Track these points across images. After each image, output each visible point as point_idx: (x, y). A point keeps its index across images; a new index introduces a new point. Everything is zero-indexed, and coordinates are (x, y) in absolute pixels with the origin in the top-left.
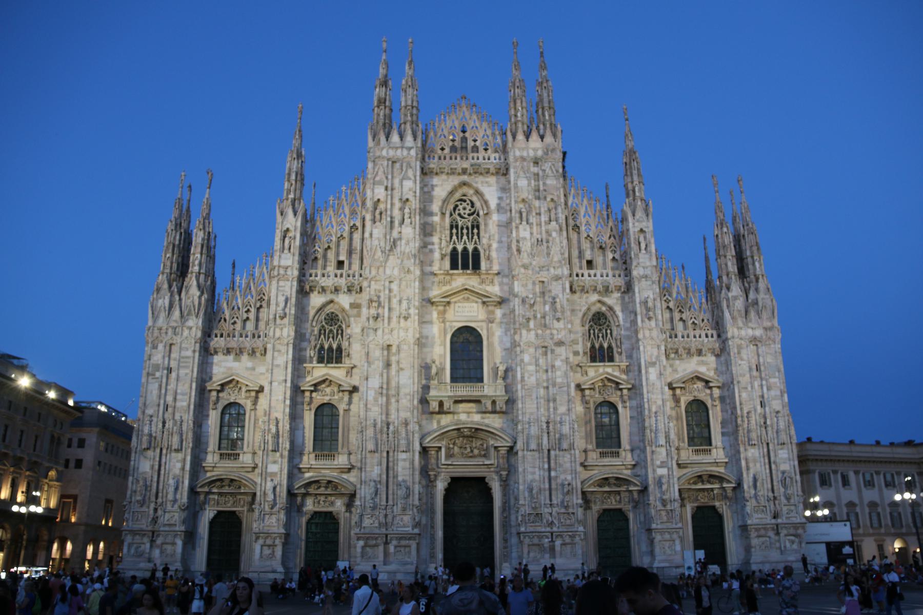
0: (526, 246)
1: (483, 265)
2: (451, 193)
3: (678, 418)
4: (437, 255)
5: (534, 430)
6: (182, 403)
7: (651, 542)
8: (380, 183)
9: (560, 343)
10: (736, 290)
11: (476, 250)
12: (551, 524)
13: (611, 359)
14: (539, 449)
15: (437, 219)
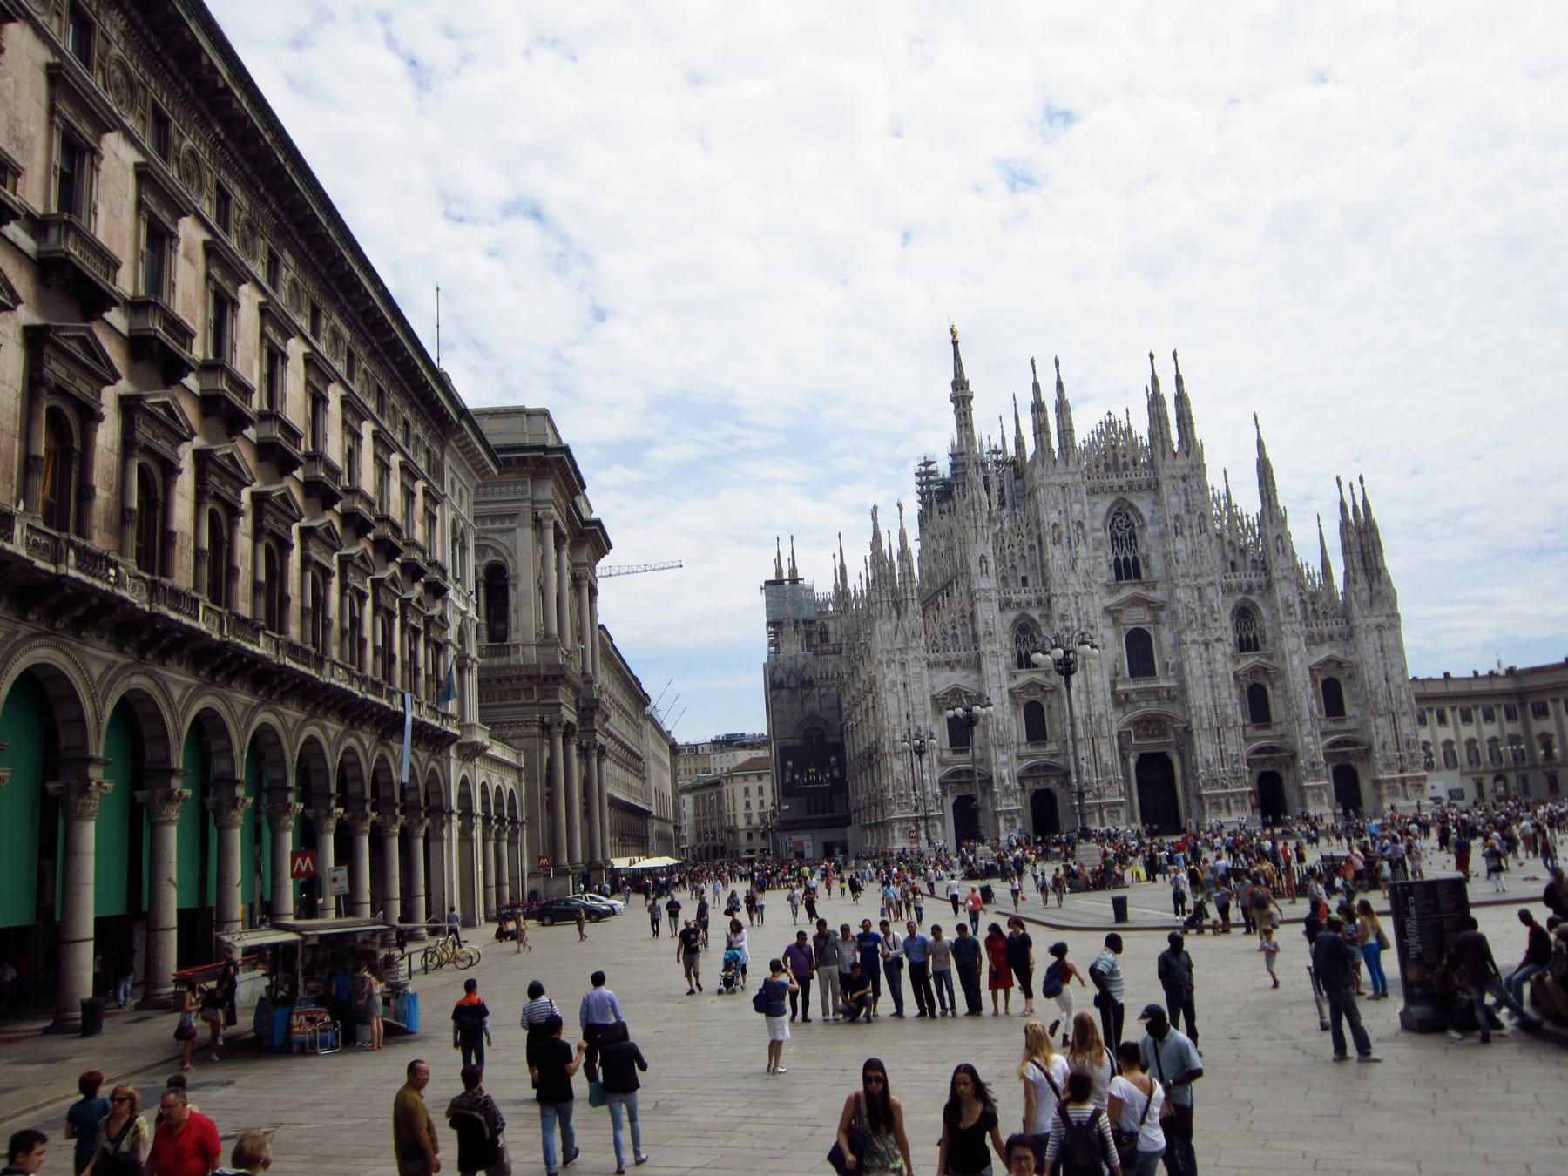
0: (1183, 556)
1: (1143, 572)
2: (1110, 510)
3: (1316, 694)
4: (1105, 567)
5: (1205, 714)
6: (919, 713)
7: (1303, 797)
8: (1055, 507)
9: (1219, 640)
10: (1362, 582)
11: (1135, 559)
12: (1226, 787)
13: (1257, 649)
14: (1211, 728)
15: (1101, 534)
